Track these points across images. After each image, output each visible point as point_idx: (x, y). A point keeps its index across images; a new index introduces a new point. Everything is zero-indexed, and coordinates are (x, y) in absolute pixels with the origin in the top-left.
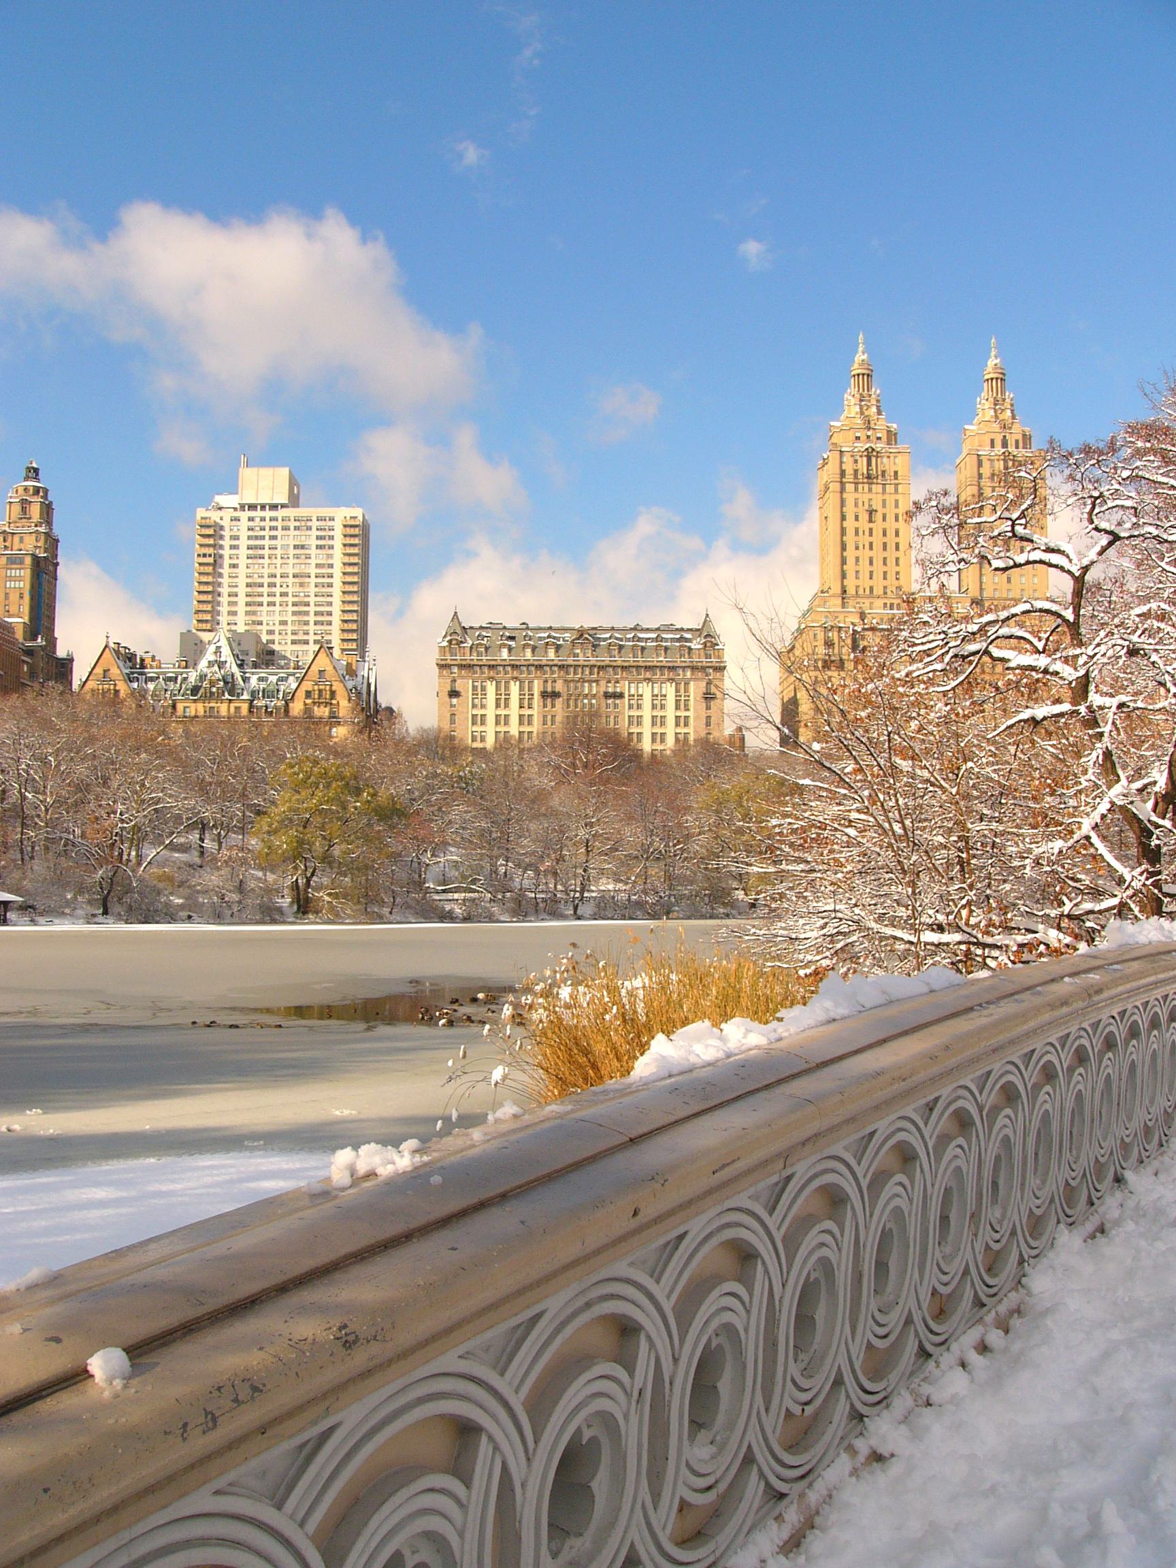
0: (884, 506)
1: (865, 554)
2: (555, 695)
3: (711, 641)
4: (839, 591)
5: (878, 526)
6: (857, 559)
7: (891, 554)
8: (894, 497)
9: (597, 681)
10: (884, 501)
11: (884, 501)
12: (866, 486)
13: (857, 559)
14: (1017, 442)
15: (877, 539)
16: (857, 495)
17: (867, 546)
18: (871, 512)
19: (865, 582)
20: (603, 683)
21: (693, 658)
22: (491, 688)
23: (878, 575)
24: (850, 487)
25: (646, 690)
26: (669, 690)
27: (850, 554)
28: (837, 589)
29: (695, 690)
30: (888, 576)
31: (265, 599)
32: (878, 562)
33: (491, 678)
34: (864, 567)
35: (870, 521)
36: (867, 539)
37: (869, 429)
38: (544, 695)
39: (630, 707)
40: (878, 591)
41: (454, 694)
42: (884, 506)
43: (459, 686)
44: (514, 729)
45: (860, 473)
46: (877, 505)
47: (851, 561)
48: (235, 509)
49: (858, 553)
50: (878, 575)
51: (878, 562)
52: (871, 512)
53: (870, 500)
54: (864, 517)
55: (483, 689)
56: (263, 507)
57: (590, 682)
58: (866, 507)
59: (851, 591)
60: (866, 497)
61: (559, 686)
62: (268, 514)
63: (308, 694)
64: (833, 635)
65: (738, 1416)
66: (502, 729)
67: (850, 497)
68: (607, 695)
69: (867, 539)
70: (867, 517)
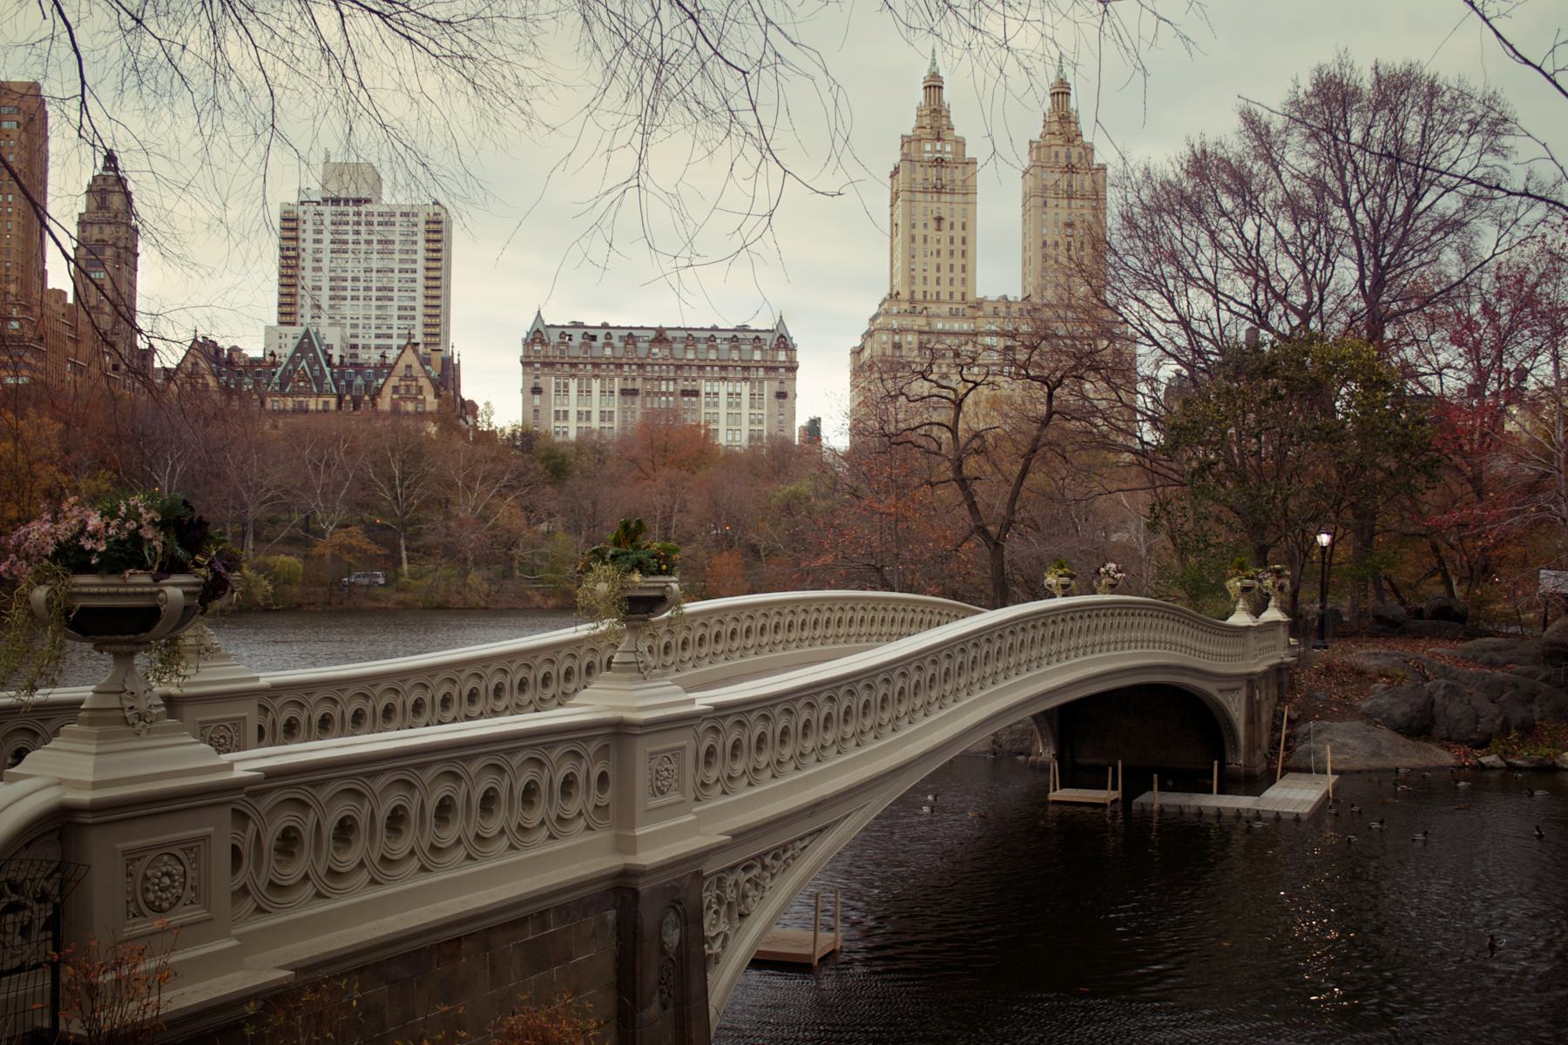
2: (634, 392)
3: (783, 342)
5: (945, 233)
9: (674, 380)
15: (945, 247)
18: (939, 219)
20: (680, 381)
21: (767, 357)
22: (573, 385)
23: (945, 281)
25: (723, 389)
26: (745, 389)
29: (769, 388)
31: (349, 294)
33: (573, 376)
35: (939, 229)
37: (939, 139)
38: (624, 392)
39: (707, 404)
40: (945, 296)
41: (537, 390)
43: (542, 382)
44: (595, 423)
48: (318, 203)
50: (945, 281)
52: (939, 219)
54: (932, 224)
55: (566, 385)
56: (347, 202)
57: (668, 380)
61: (639, 384)
62: (351, 209)
63: (396, 389)
66: (584, 424)
68: (685, 393)
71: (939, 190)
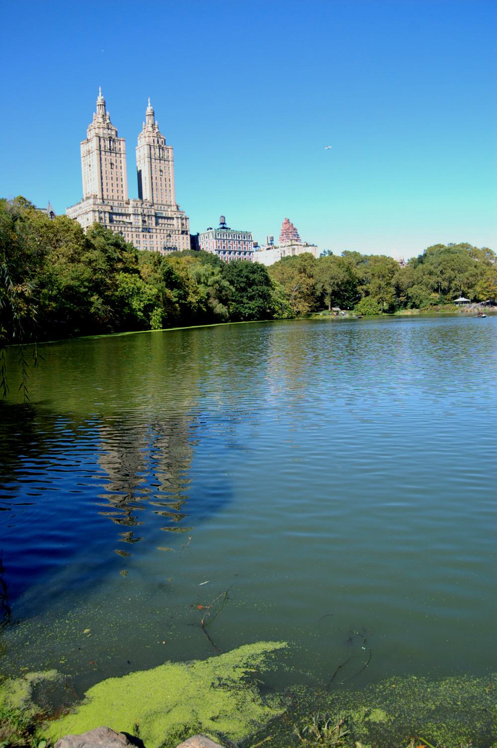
0: (116, 162)
1: (110, 182)
4: (101, 197)
6: (107, 184)
7: (120, 183)
8: (120, 159)
10: (116, 160)
11: (116, 160)
12: (109, 153)
13: (107, 184)
14: (162, 141)
16: (105, 157)
17: (110, 179)
18: (112, 164)
19: (111, 194)
23: (115, 191)
24: (103, 153)
27: (104, 181)
28: (99, 196)
30: (119, 192)
32: (115, 185)
34: (110, 188)
36: (110, 176)
40: (115, 198)
42: (116, 162)
45: (106, 147)
46: (114, 162)
47: (104, 184)
49: (107, 181)
50: (115, 191)
51: (115, 185)
53: (111, 159)
58: (110, 162)
59: (105, 197)
60: (109, 158)
64: (102, 215)
65: (339, 427)
67: (103, 157)
69: (110, 176)
70: (110, 166)
71: (111, 151)
